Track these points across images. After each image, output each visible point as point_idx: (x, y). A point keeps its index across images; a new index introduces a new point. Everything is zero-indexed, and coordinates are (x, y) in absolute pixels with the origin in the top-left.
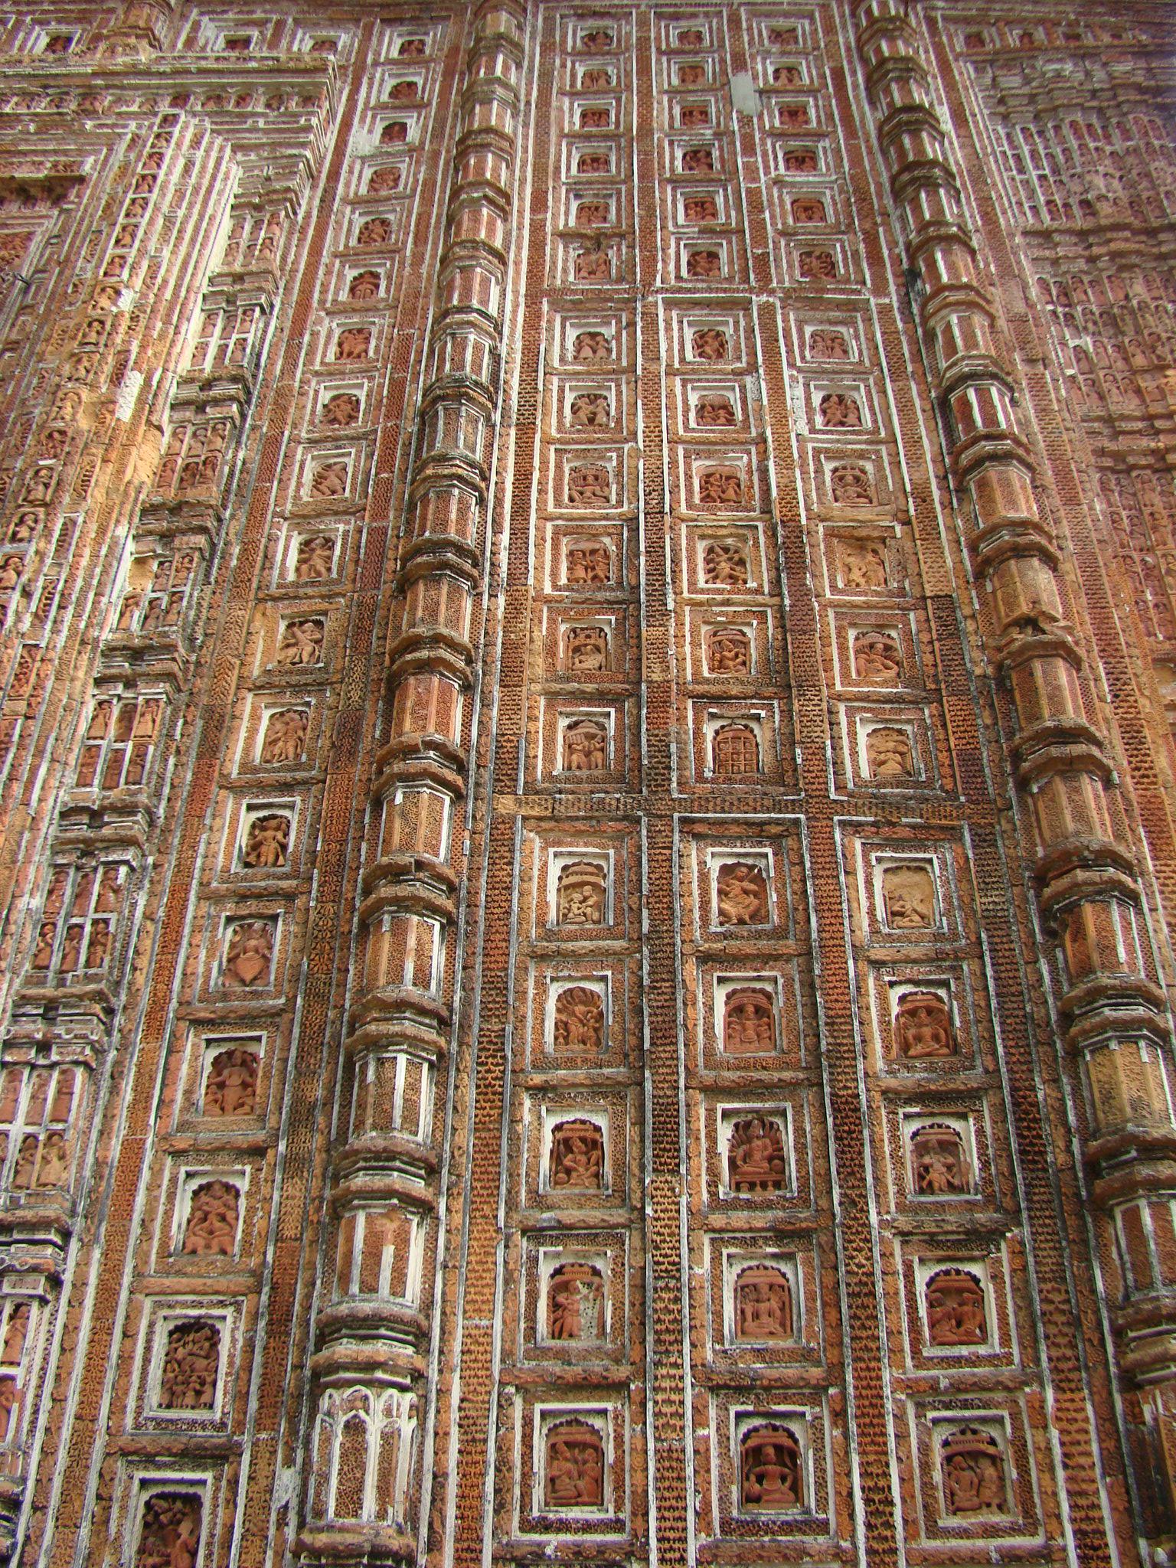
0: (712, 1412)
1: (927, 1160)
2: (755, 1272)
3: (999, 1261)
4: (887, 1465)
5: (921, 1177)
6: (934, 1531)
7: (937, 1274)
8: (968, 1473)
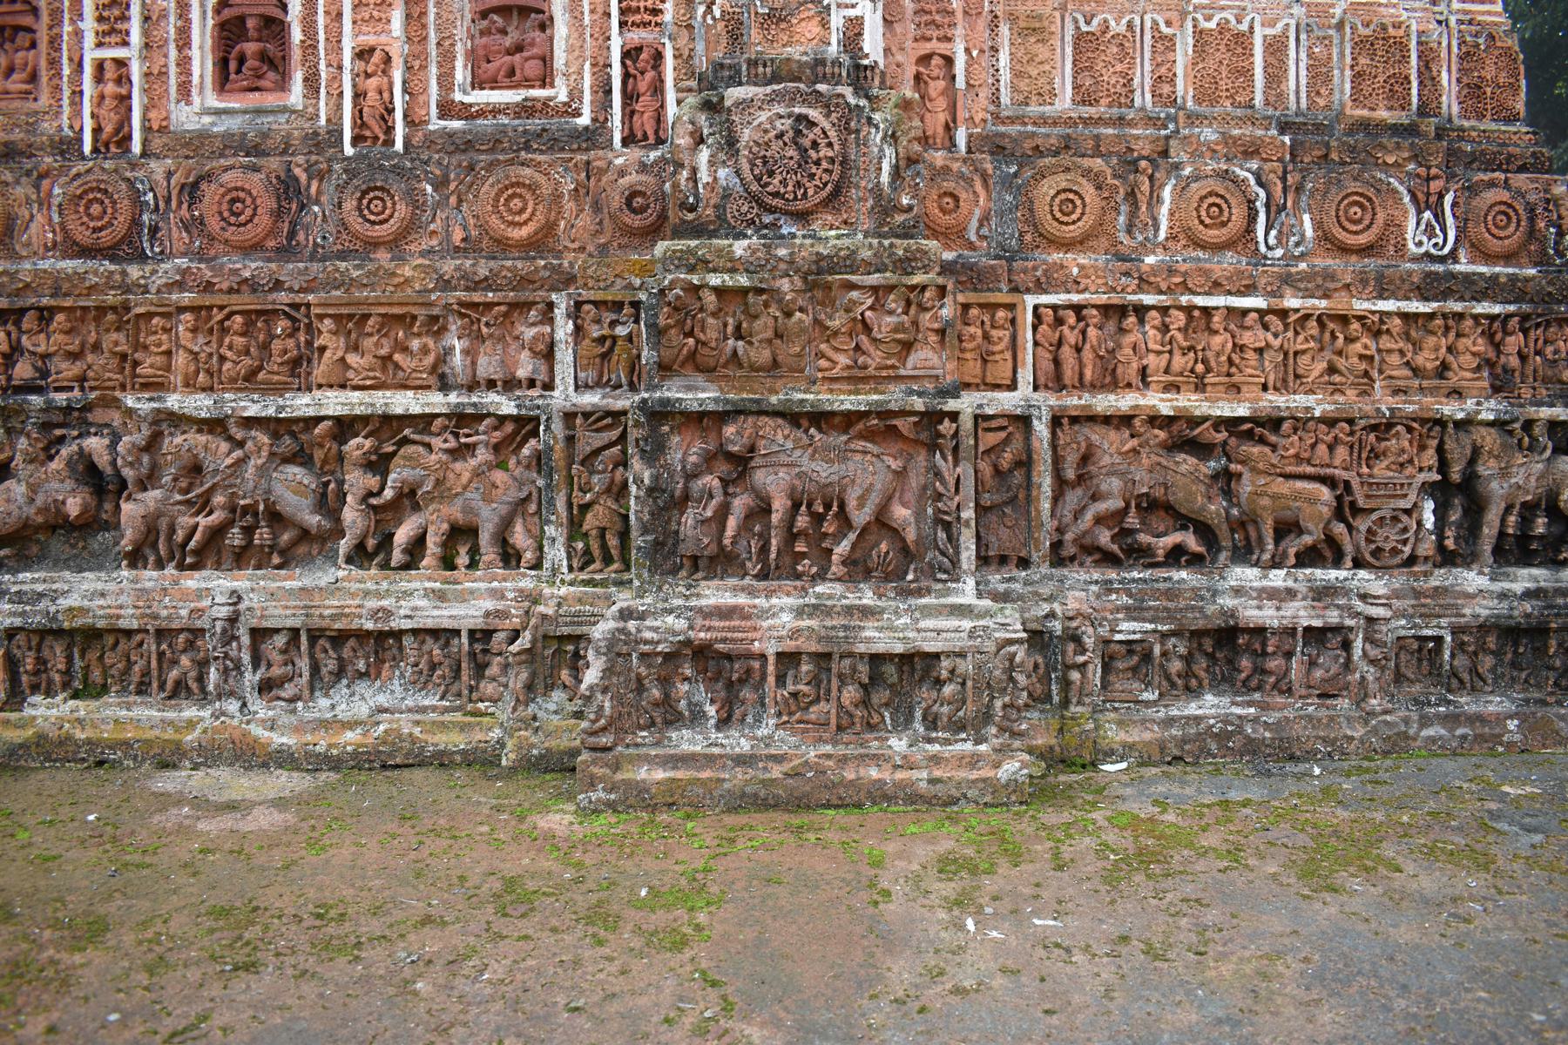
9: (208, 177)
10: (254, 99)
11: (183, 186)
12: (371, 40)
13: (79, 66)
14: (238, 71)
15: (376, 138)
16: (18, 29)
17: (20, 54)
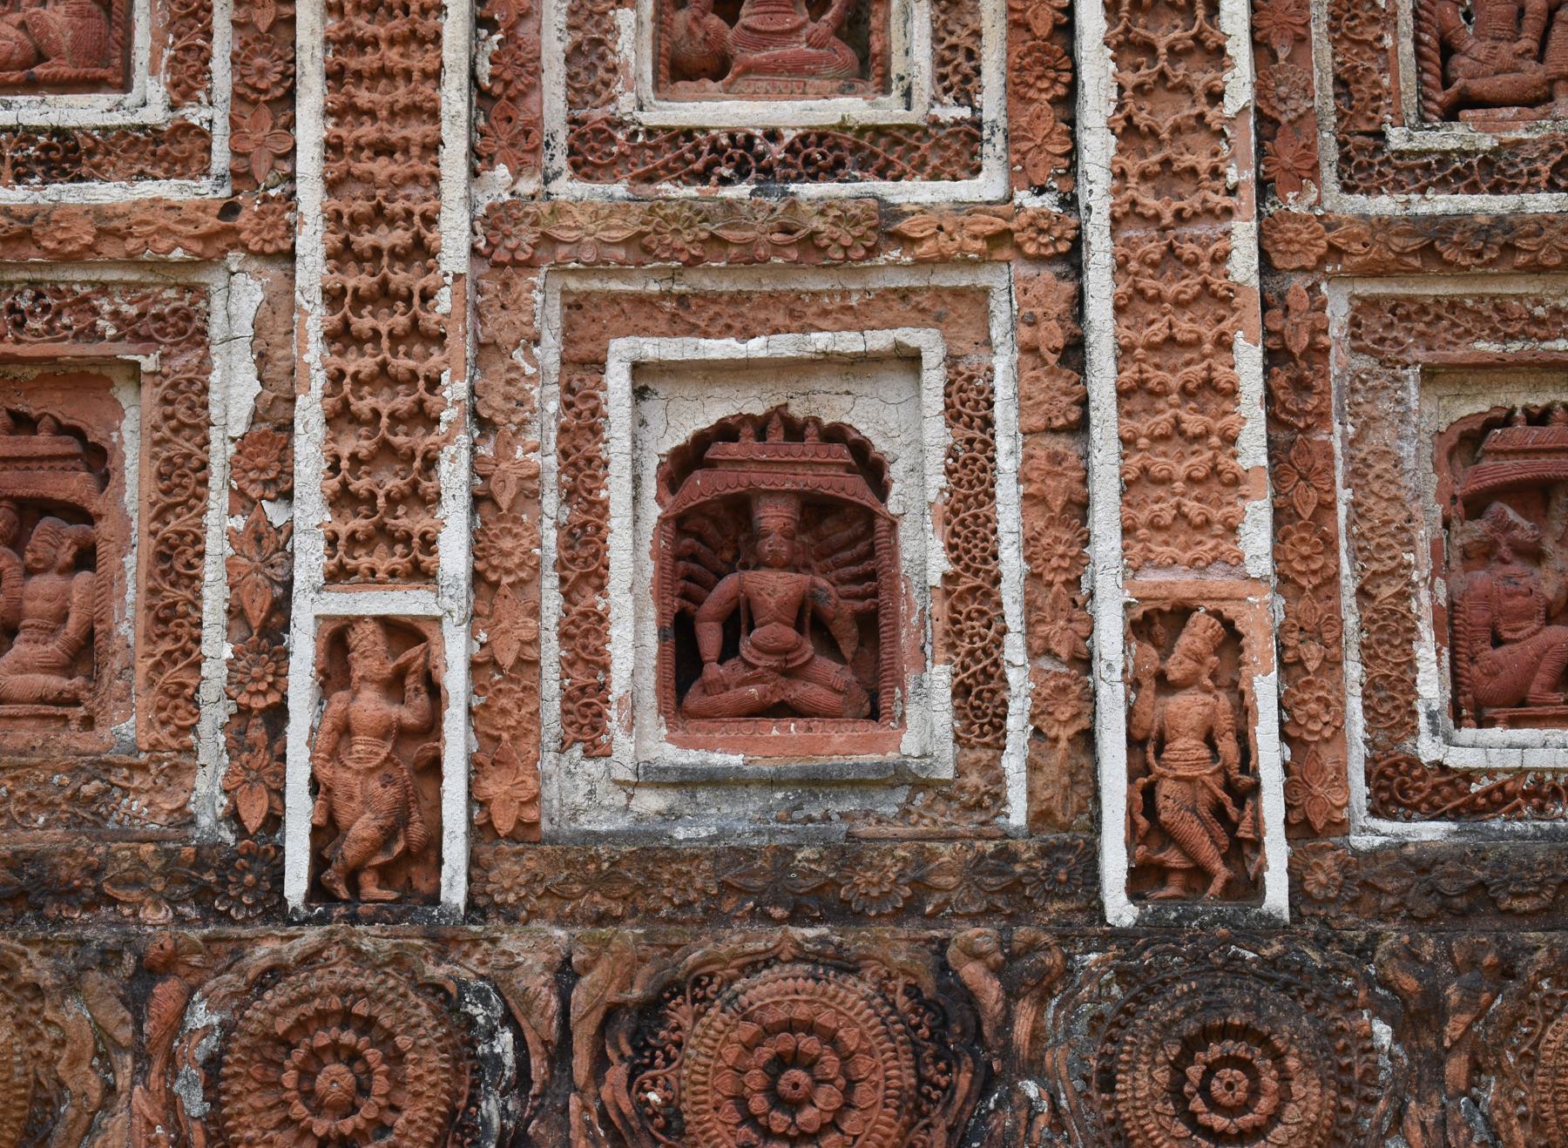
6: (1365, 165)
9: (694, 986)
10: (783, 745)
11: (611, 1013)
12: (1179, 582)
13: (266, 632)
14: (729, 650)
15: (1199, 874)
16: (32, 509)
17: (45, 584)
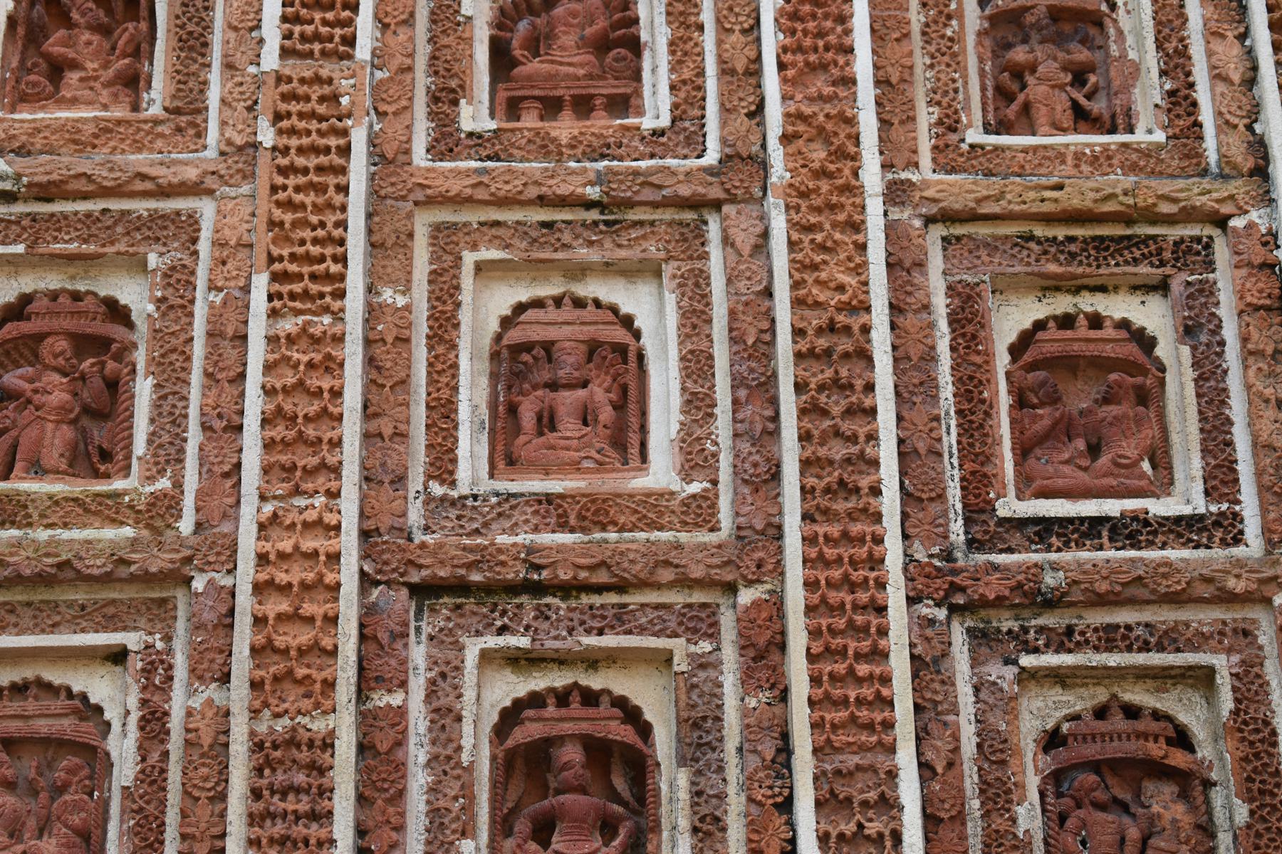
0: (418, 654)
1: (1019, 54)
2: (551, 314)
3: (1207, 291)
4: (892, 774)
5: (1005, 96)
7: (1039, 325)
8: (1106, 822)
